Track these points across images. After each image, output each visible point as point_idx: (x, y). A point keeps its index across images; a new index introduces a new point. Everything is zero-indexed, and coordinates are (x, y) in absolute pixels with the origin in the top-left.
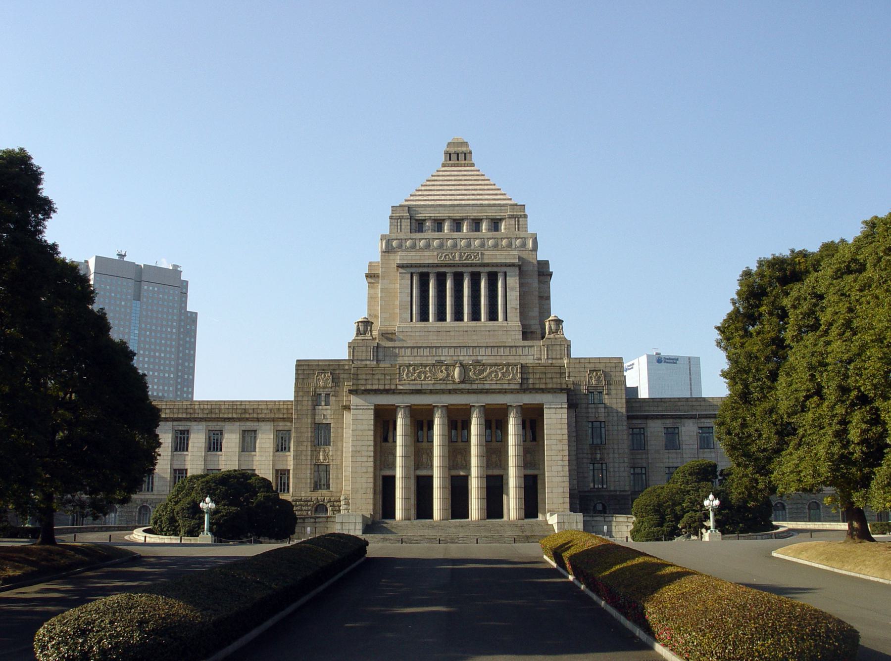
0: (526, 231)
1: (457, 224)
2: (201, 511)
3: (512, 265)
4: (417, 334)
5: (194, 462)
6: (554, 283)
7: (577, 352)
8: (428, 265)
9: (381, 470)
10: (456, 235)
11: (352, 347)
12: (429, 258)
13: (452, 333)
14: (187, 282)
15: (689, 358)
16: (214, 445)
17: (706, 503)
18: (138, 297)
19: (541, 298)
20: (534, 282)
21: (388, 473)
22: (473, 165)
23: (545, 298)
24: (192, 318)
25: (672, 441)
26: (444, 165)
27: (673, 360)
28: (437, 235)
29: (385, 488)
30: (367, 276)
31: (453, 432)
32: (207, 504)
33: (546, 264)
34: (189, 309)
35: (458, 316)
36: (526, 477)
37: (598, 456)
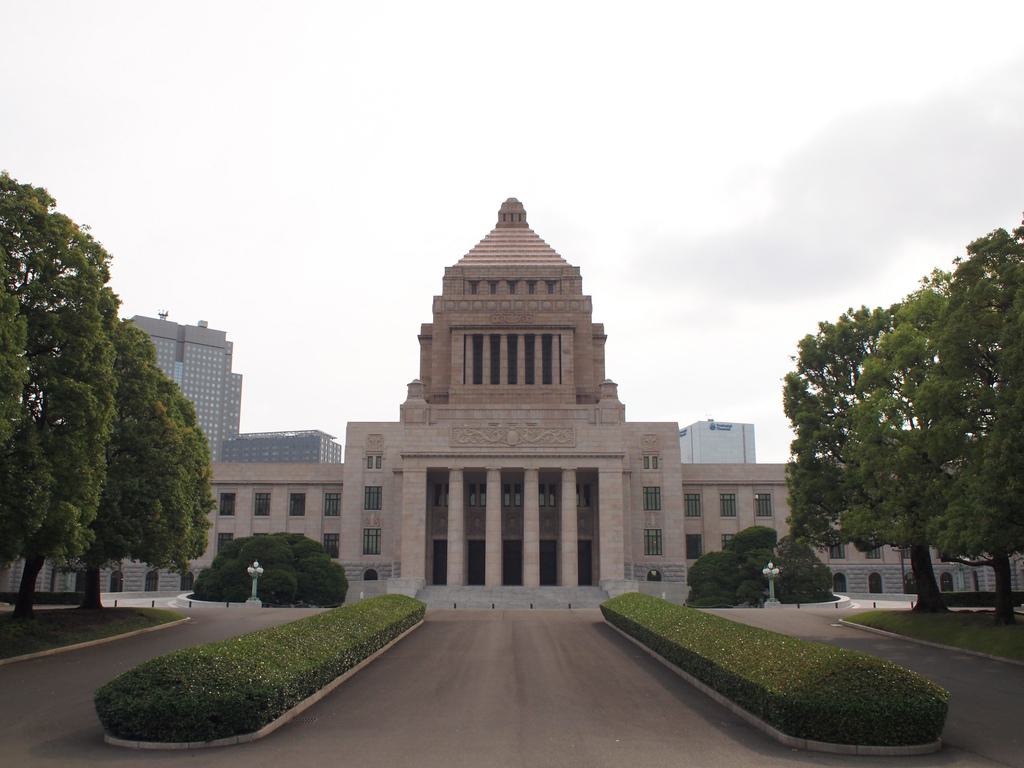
0: (581, 293)
1: (512, 284)
2: (249, 577)
3: (567, 328)
4: (471, 397)
5: (243, 524)
6: (608, 346)
7: (631, 416)
8: (482, 328)
9: (432, 534)
10: (510, 297)
11: (403, 408)
12: (482, 319)
13: (505, 396)
14: (232, 343)
15: (743, 426)
16: (262, 507)
17: (765, 571)
18: (180, 357)
21: (442, 537)
22: (527, 225)
23: (600, 361)
24: (238, 379)
25: (728, 507)
26: (498, 226)
27: (727, 427)
28: (490, 296)
30: (420, 338)
31: (507, 496)
32: (255, 569)
33: (600, 327)
34: (233, 371)
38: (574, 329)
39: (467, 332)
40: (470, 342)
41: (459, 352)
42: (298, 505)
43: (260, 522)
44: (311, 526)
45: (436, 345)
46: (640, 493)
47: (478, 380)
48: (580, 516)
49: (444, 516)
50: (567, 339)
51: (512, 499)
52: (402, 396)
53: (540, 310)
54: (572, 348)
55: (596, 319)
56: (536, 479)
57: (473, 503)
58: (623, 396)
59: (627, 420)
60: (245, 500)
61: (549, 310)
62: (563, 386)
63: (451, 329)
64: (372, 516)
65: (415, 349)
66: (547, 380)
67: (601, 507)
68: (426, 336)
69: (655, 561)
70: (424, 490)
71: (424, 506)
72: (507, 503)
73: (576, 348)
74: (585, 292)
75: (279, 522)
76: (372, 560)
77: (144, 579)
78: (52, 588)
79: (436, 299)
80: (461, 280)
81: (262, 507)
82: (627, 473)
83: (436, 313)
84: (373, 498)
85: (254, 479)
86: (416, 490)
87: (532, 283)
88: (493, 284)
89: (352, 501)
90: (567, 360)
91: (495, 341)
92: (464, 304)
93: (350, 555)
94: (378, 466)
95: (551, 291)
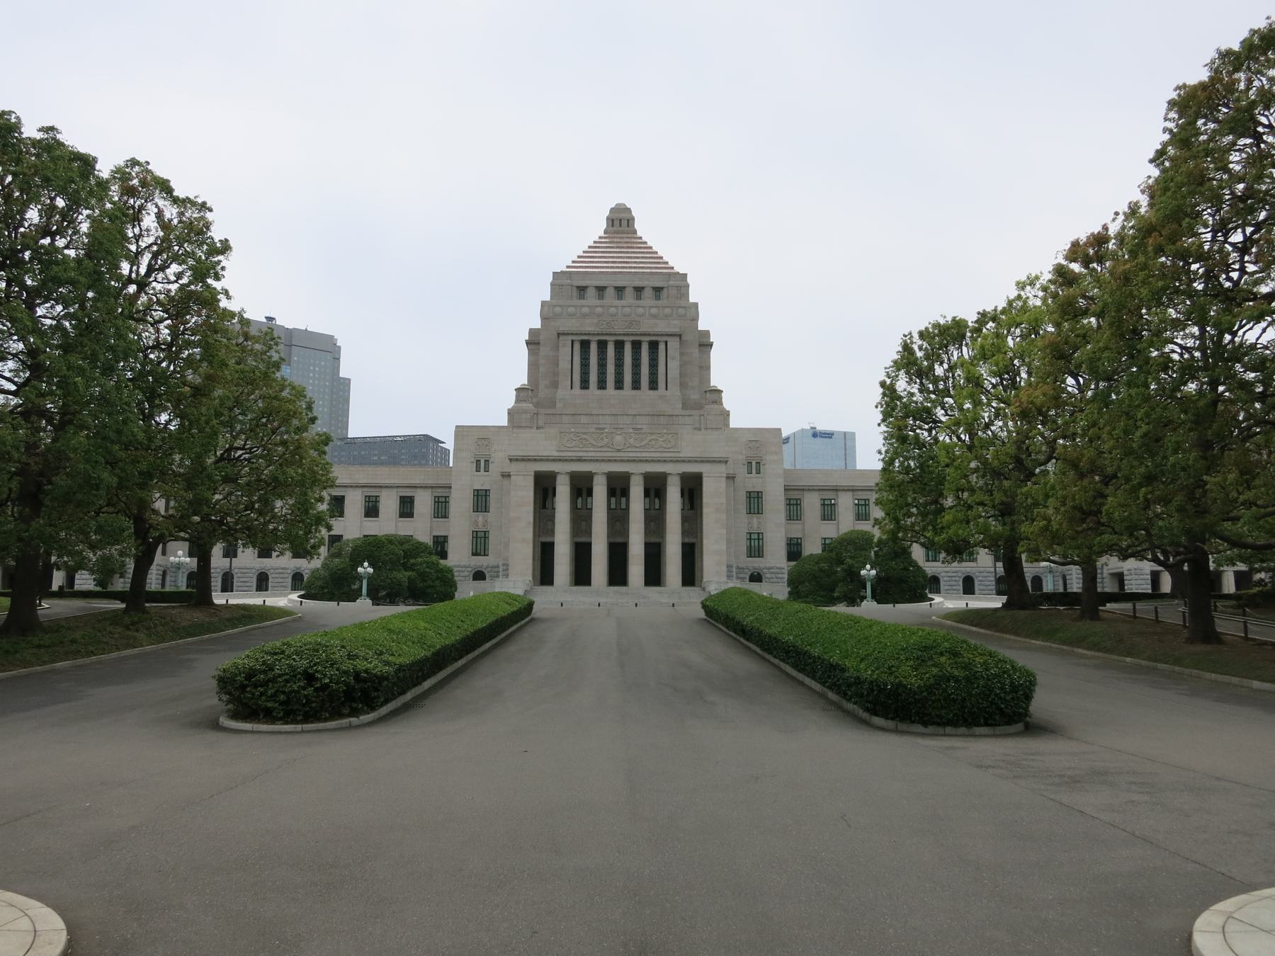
5: (352, 526)
6: (714, 353)
7: (733, 423)
10: (617, 302)
11: (510, 412)
12: (589, 326)
16: (372, 510)
19: (701, 367)
20: (695, 351)
21: (549, 539)
23: (707, 368)
24: (347, 382)
25: (829, 512)
28: (598, 302)
29: (545, 554)
31: (613, 500)
32: (365, 569)
33: (707, 333)
35: (619, 385)
36: (684, 545)
37: (755, 525)
38: (680, 336)
39: (574, 338)
40: (577, 347)
41: (567, 358)
42: (407, 508)
43: (369, 524)
44: (420, 529)
45: (544, 351)
46: (743, 497)
47: (585, 384)
48: (685, 520)
49: (552, 519)
50: (674, 344)
51: (618, 503)
52: (510, 401)
53: (647, 318)
54: (677, 355)
55: (702, 326)
56: (642, 482)
57: (579, 506)
58: (727, 403)
59: (731, 426)
60: (354, 504)
61: (655, 316)
62: (668, 393)
63: (559, 335)
64: (480, 519)
65: (522, 355)
66: (653, 385)
67: (705, 511)
68: (533, 342)
69: (756, 563)
70: (532, 493)
71: (531, 508)
72: (613, 506)
73: (682, 354)
74: (692, 300)
75: (388, 524)
76: (480, 562)
77: (255, 580)
78: (163, 585)
79: (544, 304)
80: (570, 287)
81: (372, 510)
82: (731, 478)
83: (544, 318)
84: (481, 500)
85: (363, 481)
86: (524, 493)
87: (639, 290)
88: (601, 290)
89: (460, 503)
90: (674, 366)
91: (602, 345)
92: (571, 310)
93: (459, 557)
94: (486, 470)
95: (658, 298)
